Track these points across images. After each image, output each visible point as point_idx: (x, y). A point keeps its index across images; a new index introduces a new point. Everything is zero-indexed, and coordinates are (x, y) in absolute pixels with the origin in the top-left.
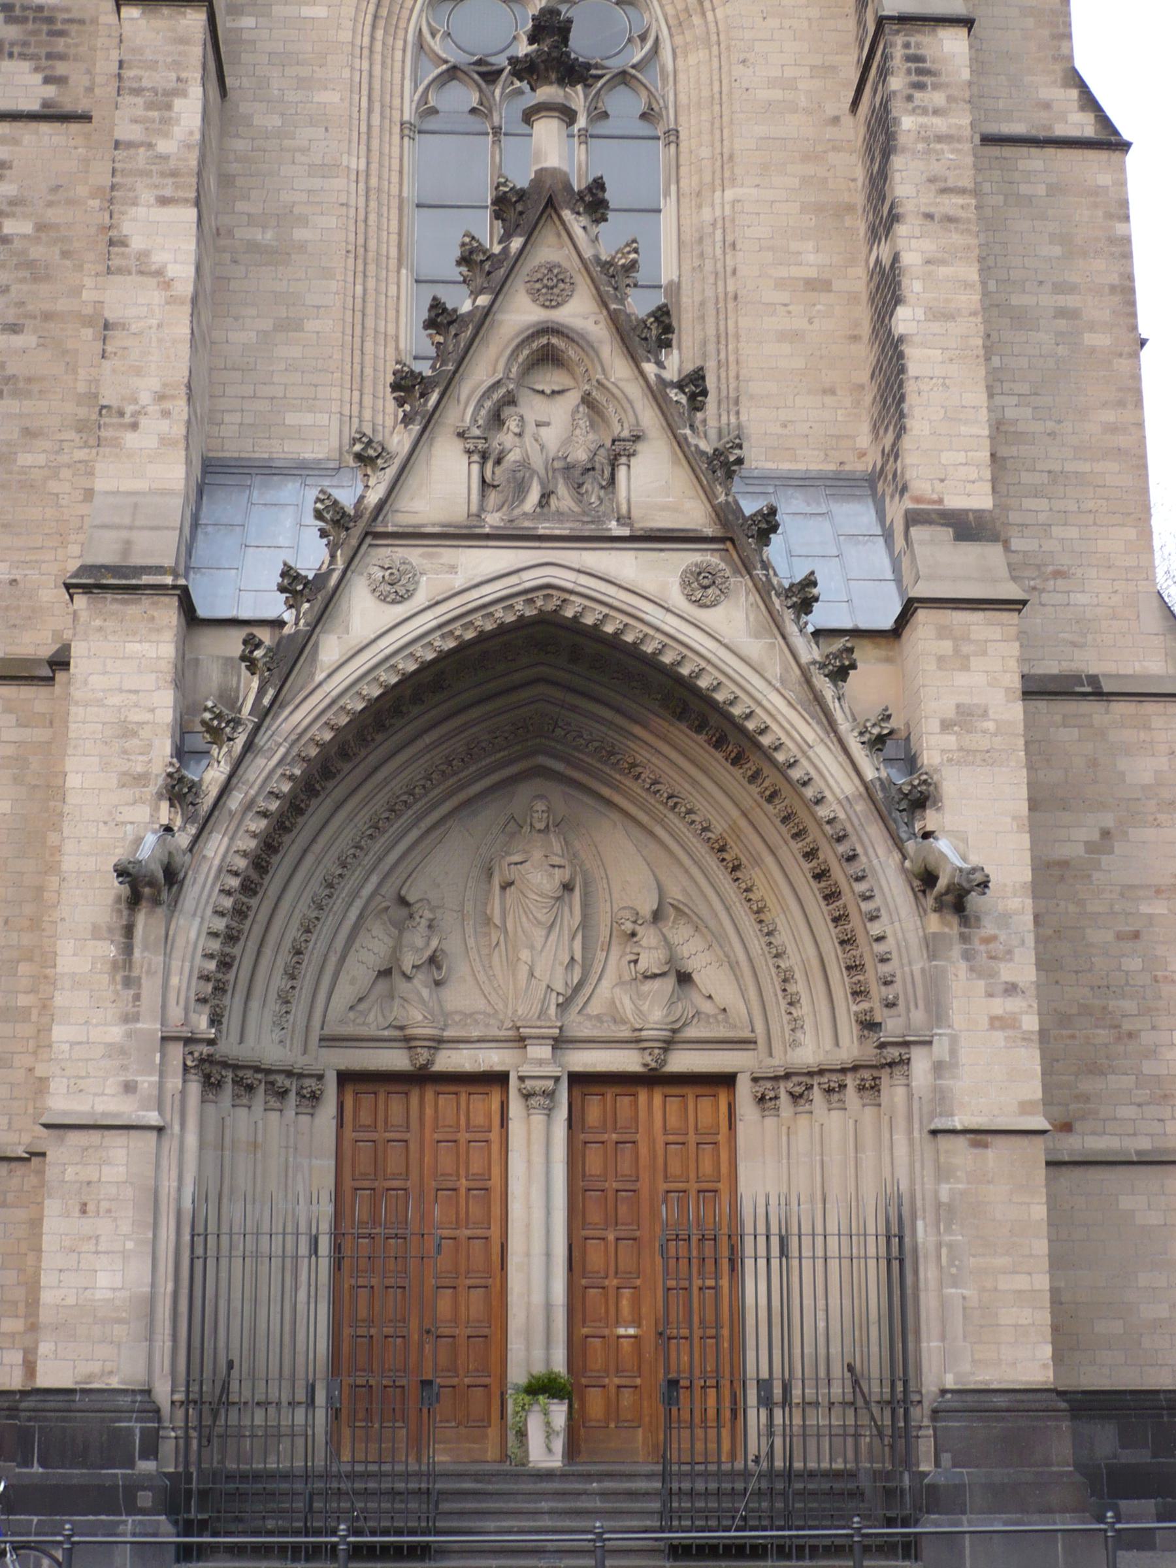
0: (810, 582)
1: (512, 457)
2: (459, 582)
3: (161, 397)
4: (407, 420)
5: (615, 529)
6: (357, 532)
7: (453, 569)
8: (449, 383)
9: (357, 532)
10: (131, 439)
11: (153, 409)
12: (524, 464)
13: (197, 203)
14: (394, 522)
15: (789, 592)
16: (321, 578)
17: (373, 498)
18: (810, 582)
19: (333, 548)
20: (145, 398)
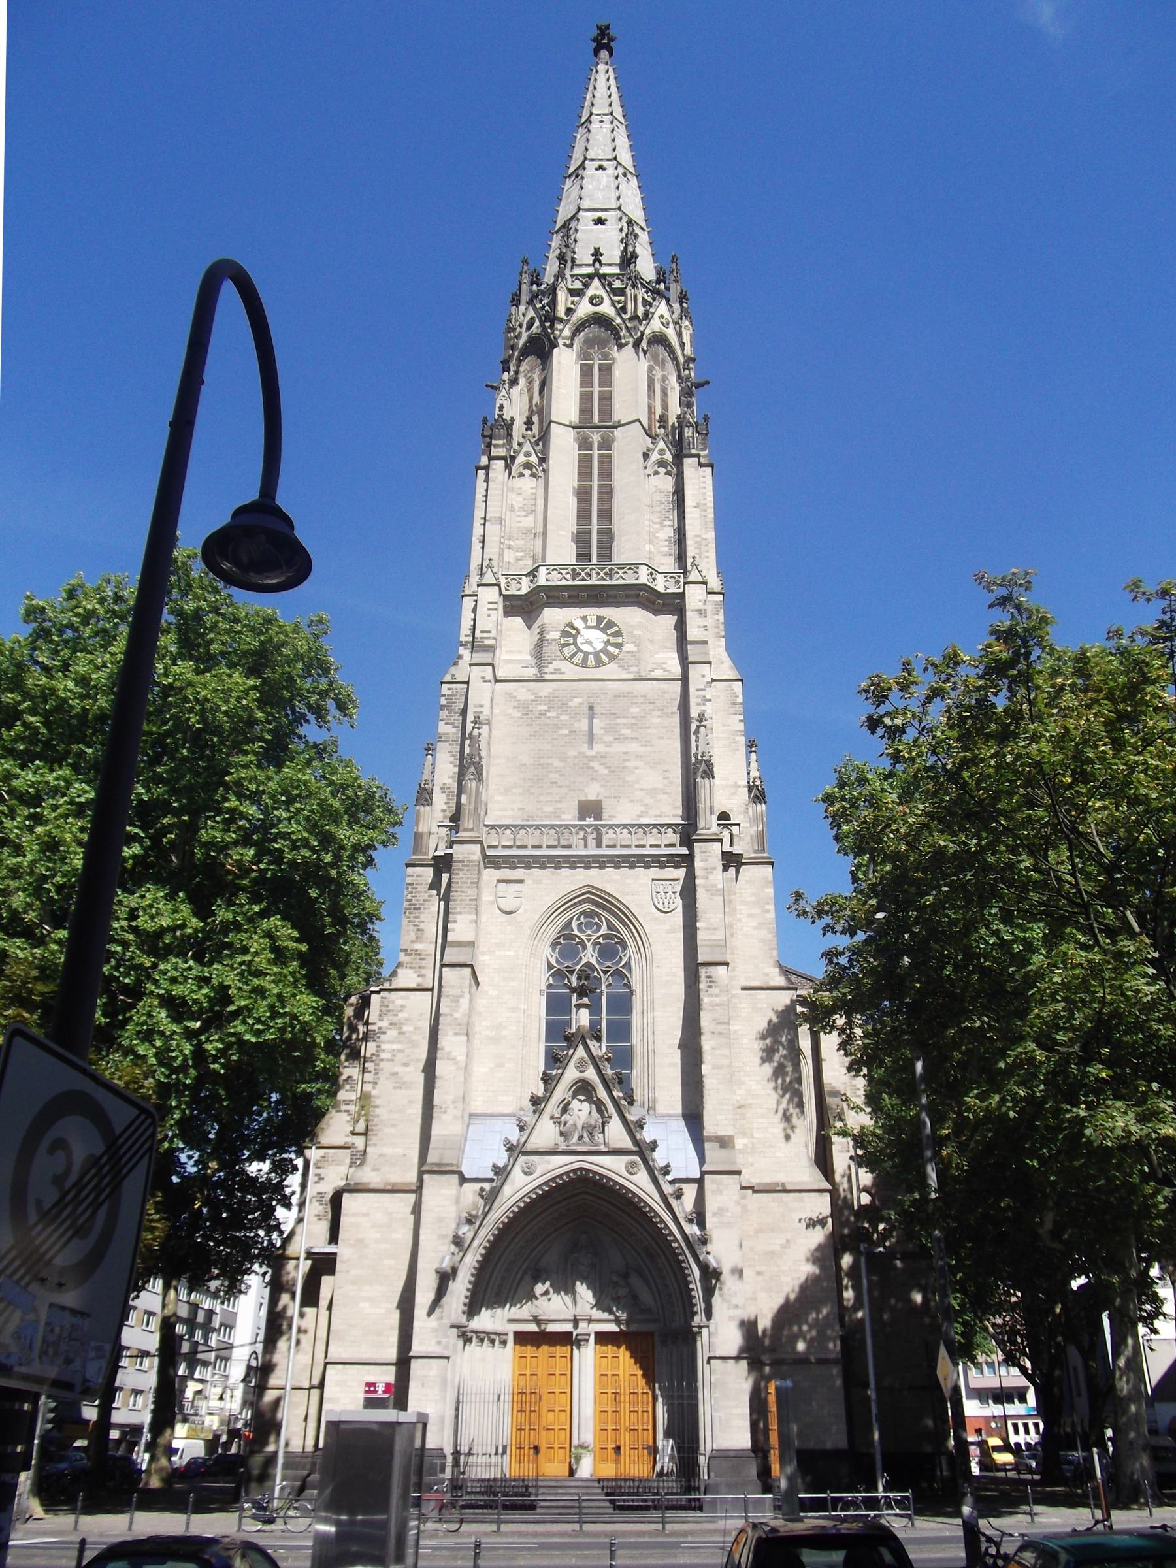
0: (668, 1166)
1: (570, 1122)
2: (551, 1167)
3: (454, 1102)
4: (535, 1112)
5: (603, 1148)
6: (518, 1151)
7: (549, 1163)
8: (546, 1098)
9: (518, 1151)
10: (444, 1117)
11: (452, 1106)
12: (575, 1125)
13: (467, 1035)
14: (529, 1146)
15: (661, 1169)
16: (505, 1167)
17: (523, 1140)
18: (668, 1166)
19: (510, 1156)
20: (449, 1102)
